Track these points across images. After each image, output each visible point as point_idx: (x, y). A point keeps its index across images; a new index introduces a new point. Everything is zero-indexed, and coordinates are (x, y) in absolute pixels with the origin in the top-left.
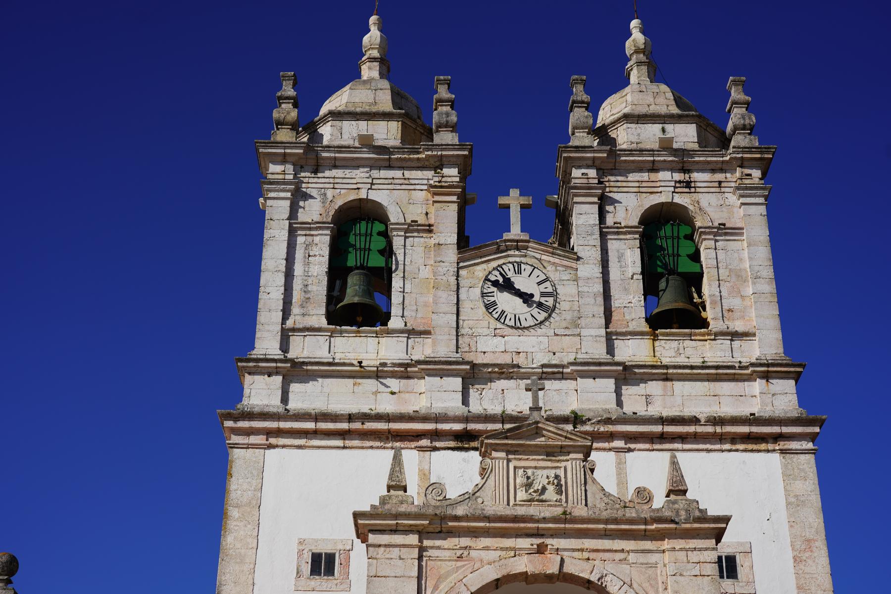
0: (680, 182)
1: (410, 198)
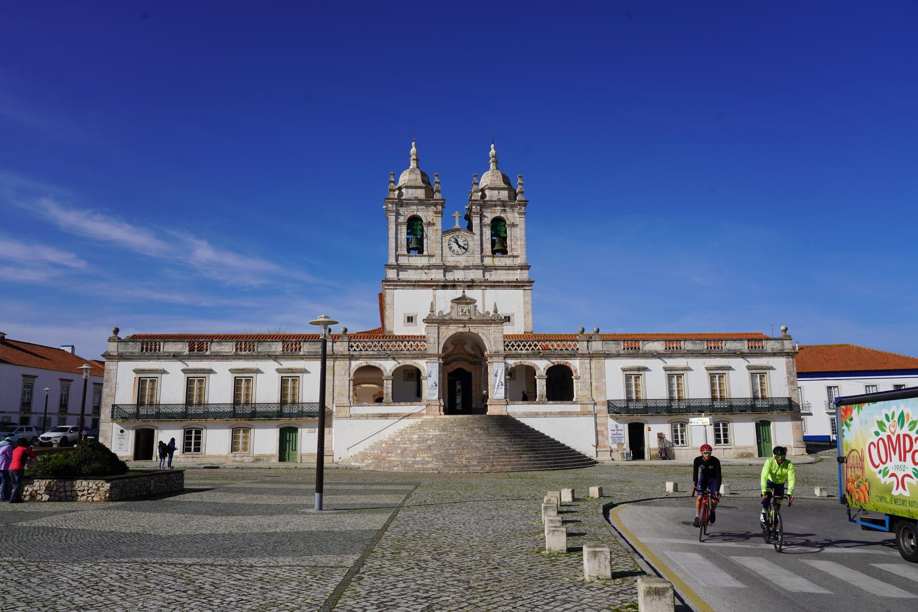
1: (426, 214)
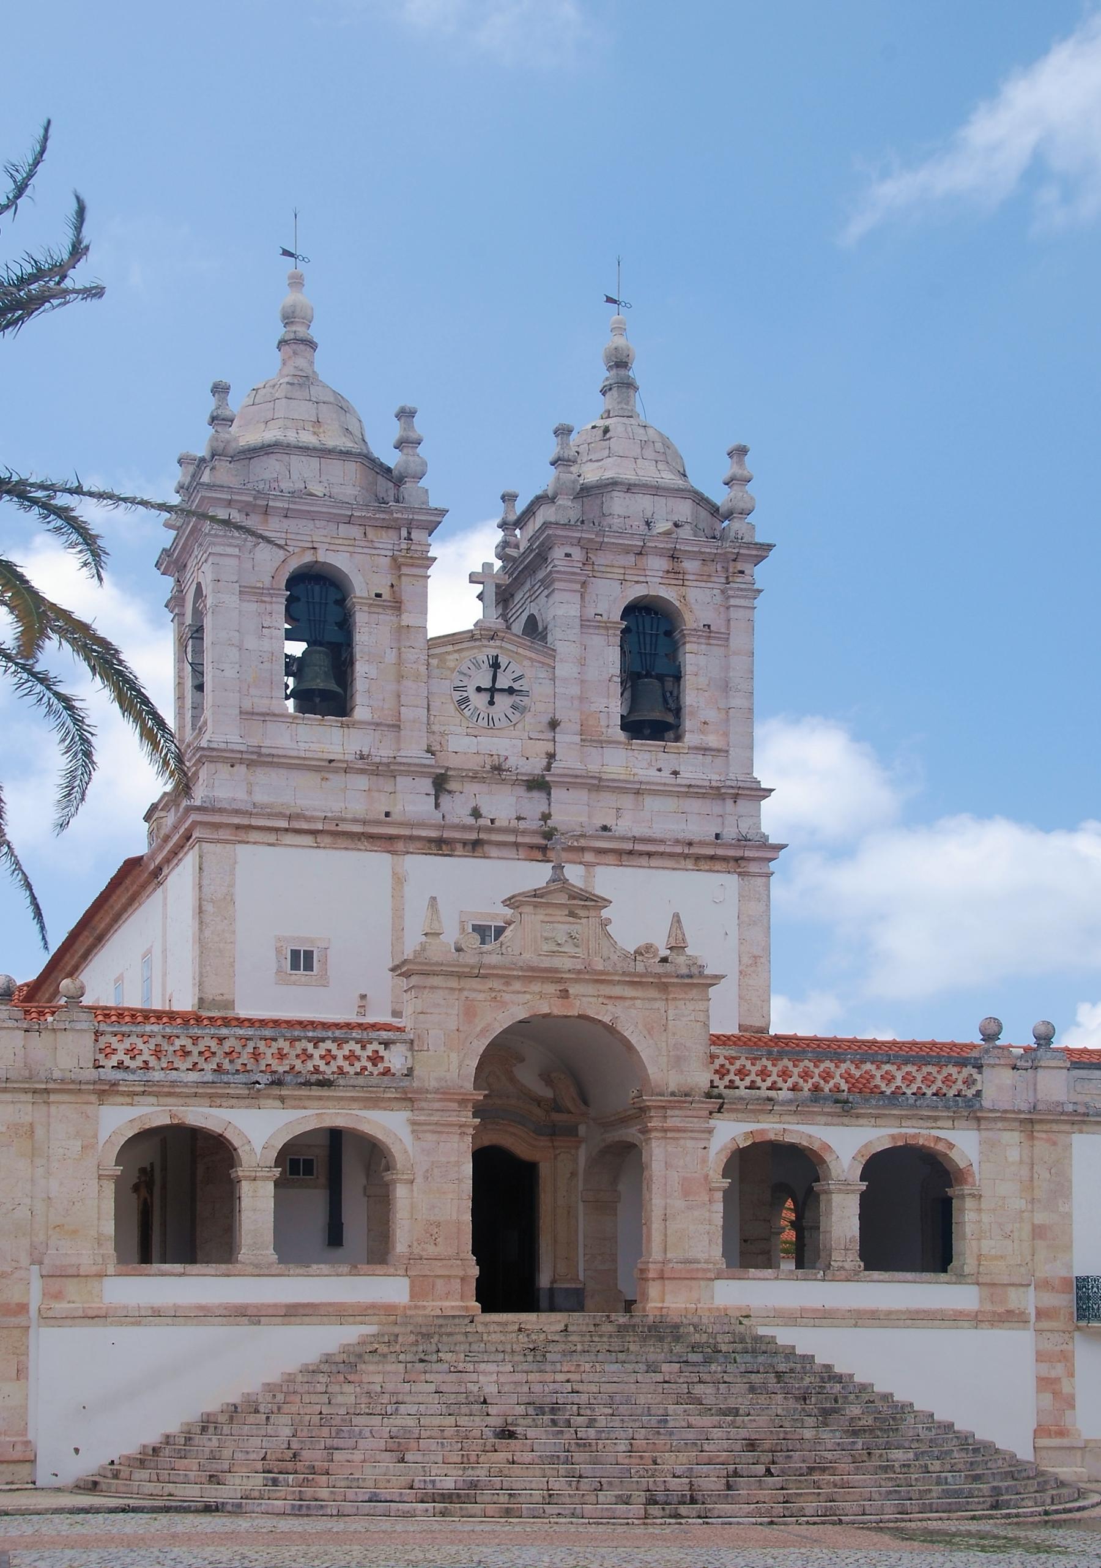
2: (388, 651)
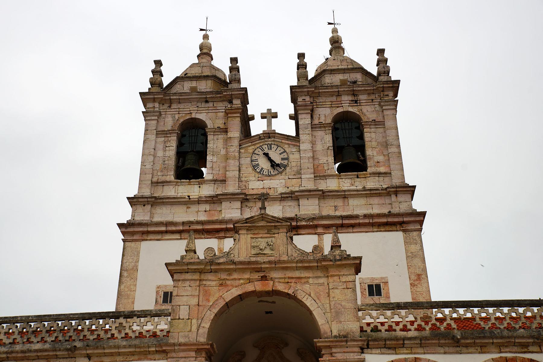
0: (352, 101)
2: (222, 149)
